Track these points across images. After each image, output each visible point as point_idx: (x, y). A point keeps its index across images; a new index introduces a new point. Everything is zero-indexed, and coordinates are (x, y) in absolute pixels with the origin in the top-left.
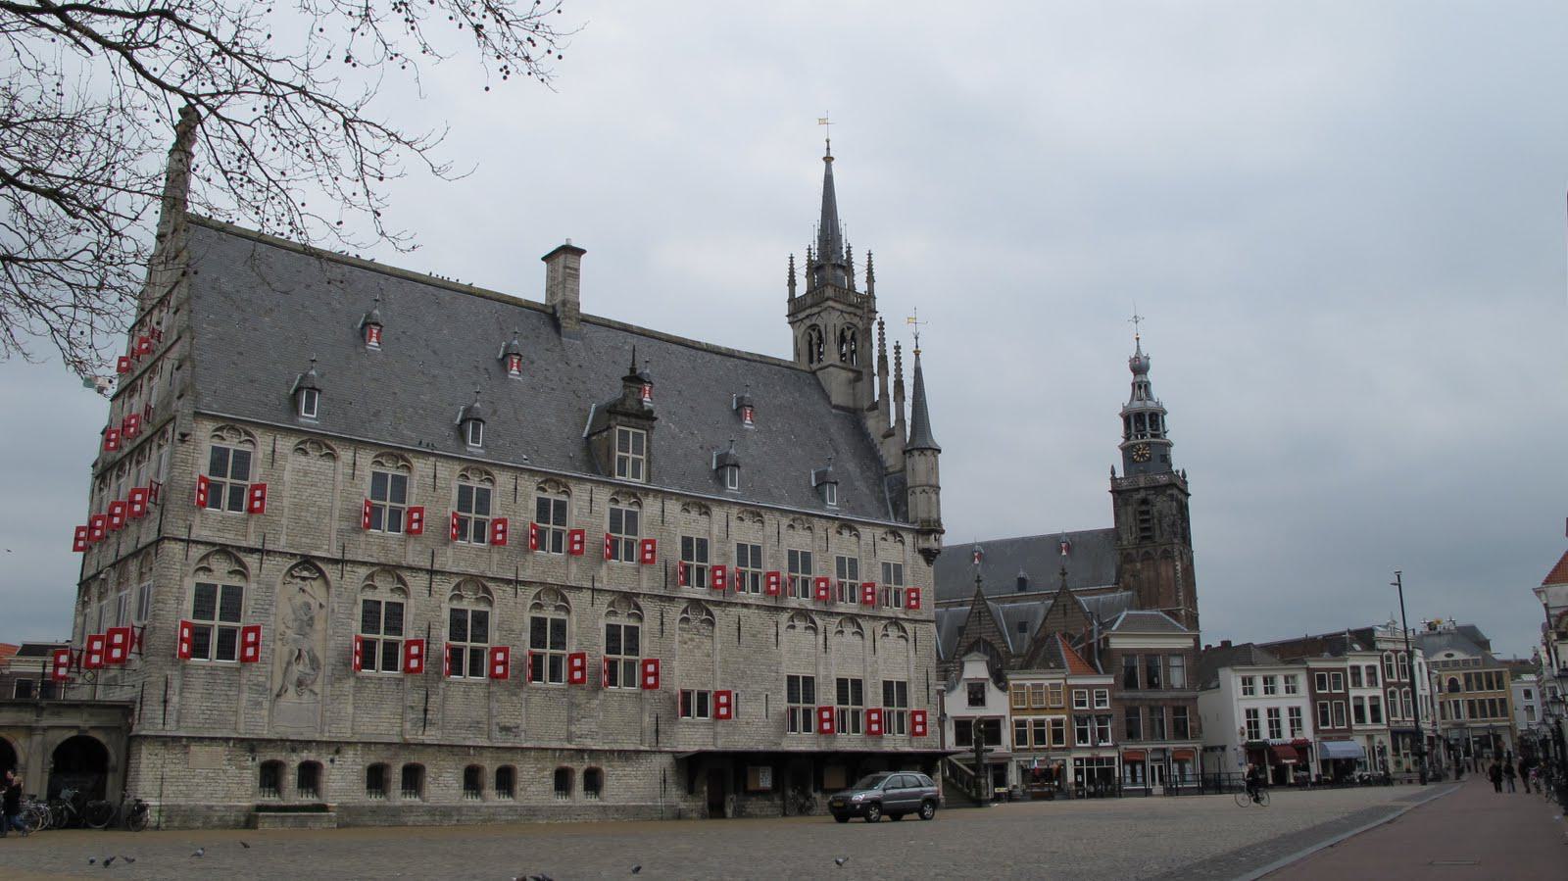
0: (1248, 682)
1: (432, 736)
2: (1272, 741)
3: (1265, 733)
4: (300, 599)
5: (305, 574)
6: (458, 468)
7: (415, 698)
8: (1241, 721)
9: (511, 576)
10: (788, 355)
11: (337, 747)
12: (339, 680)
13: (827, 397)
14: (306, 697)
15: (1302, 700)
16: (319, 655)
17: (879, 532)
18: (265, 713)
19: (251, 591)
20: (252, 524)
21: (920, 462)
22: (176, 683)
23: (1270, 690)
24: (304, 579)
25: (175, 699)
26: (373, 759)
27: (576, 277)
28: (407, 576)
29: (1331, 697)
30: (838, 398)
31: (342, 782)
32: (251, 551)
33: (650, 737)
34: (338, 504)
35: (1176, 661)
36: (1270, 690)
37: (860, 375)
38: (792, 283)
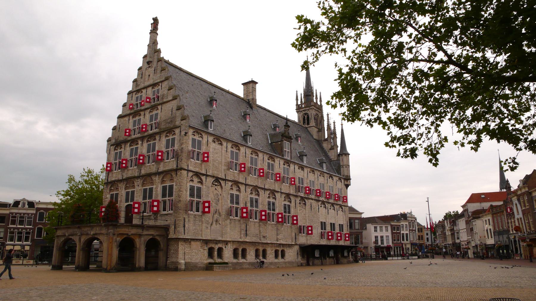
0: (375, 228)
1: (248, 239)
2: (382, 245)
3: (380, 243)
4: (216, 192)
5: (216, 184)
6: (250, 151)
7: (243, 226)
8: (374, 240)
9: (263, 187)
10: (297, 121)
11: (226, 242)
12: (226, 220)
13: (312, 136)
14: (218, 225)
15: (389, 233)
16: (220, 211)
17: (337, 178)
18: (209, 230)
19: (204, 188)
20: (203, 166)
21: (344, 157)
22: (187, 220)
23: (381, 230)
24: (216, 185)
25: (186, 226)
26: (235, 247)
27: (255, 91)
28: (240, 185)
29: (397, 233)
30: (315, 137)
31: (228, 254)
32: (203, 175)
33: (294, 240)
34: (223, 161)
35: (357, 221)
36: (381, 230)
37: (321, 130)
38: (297, 99)
